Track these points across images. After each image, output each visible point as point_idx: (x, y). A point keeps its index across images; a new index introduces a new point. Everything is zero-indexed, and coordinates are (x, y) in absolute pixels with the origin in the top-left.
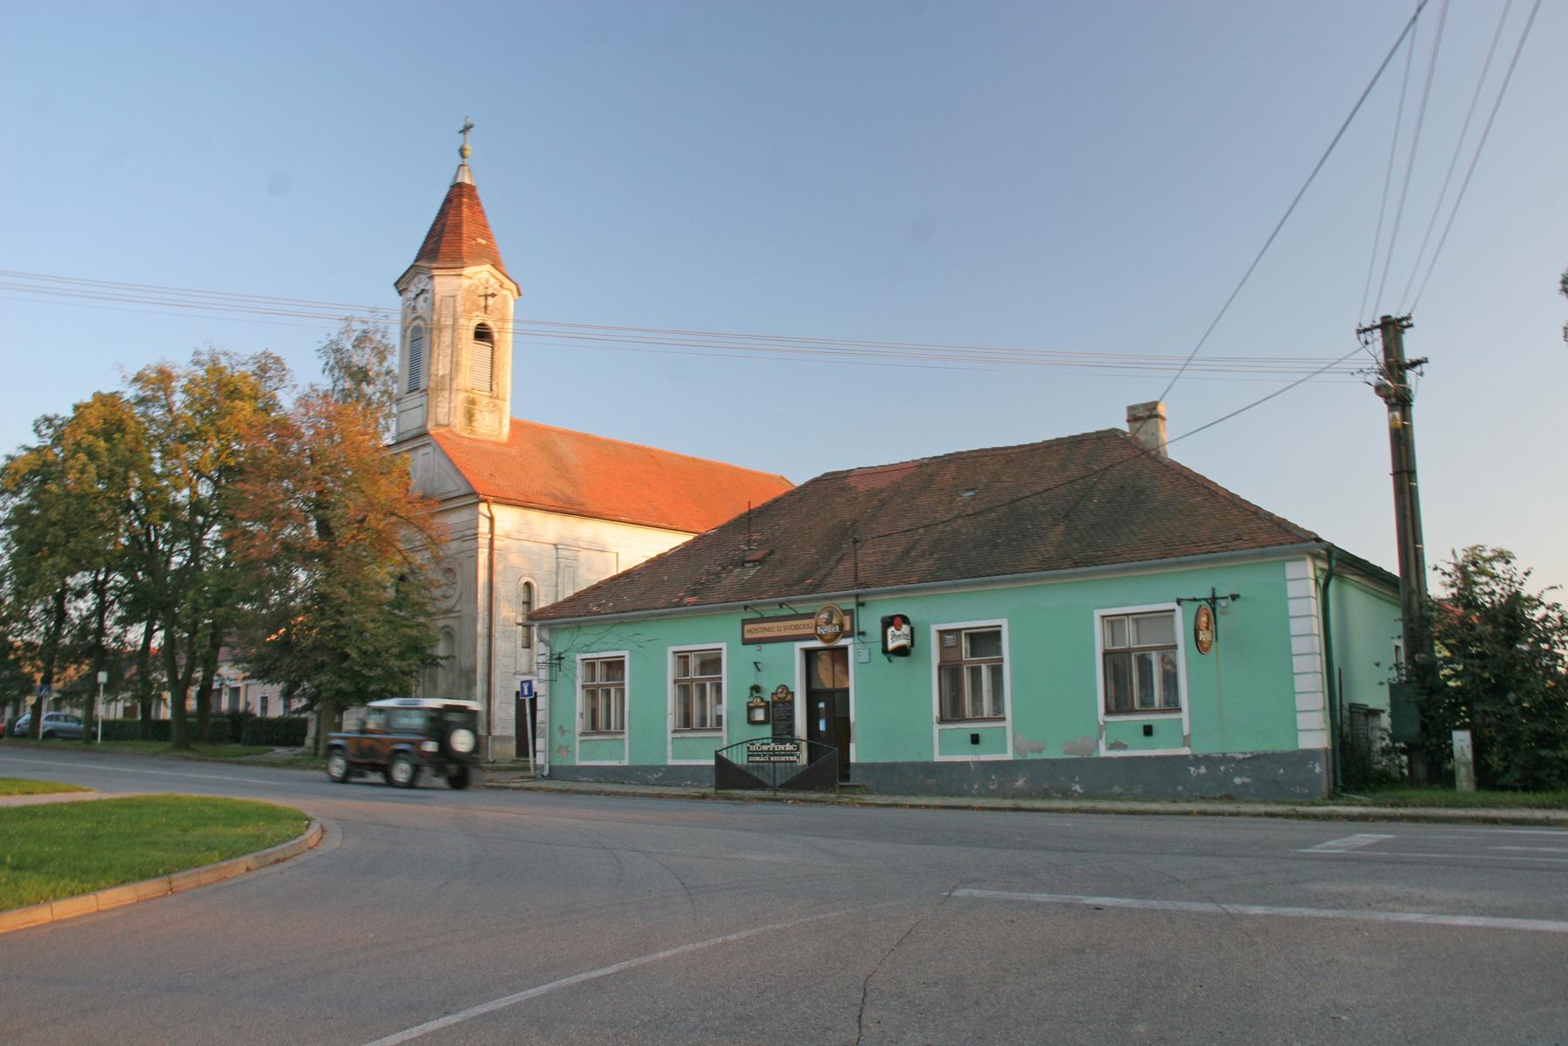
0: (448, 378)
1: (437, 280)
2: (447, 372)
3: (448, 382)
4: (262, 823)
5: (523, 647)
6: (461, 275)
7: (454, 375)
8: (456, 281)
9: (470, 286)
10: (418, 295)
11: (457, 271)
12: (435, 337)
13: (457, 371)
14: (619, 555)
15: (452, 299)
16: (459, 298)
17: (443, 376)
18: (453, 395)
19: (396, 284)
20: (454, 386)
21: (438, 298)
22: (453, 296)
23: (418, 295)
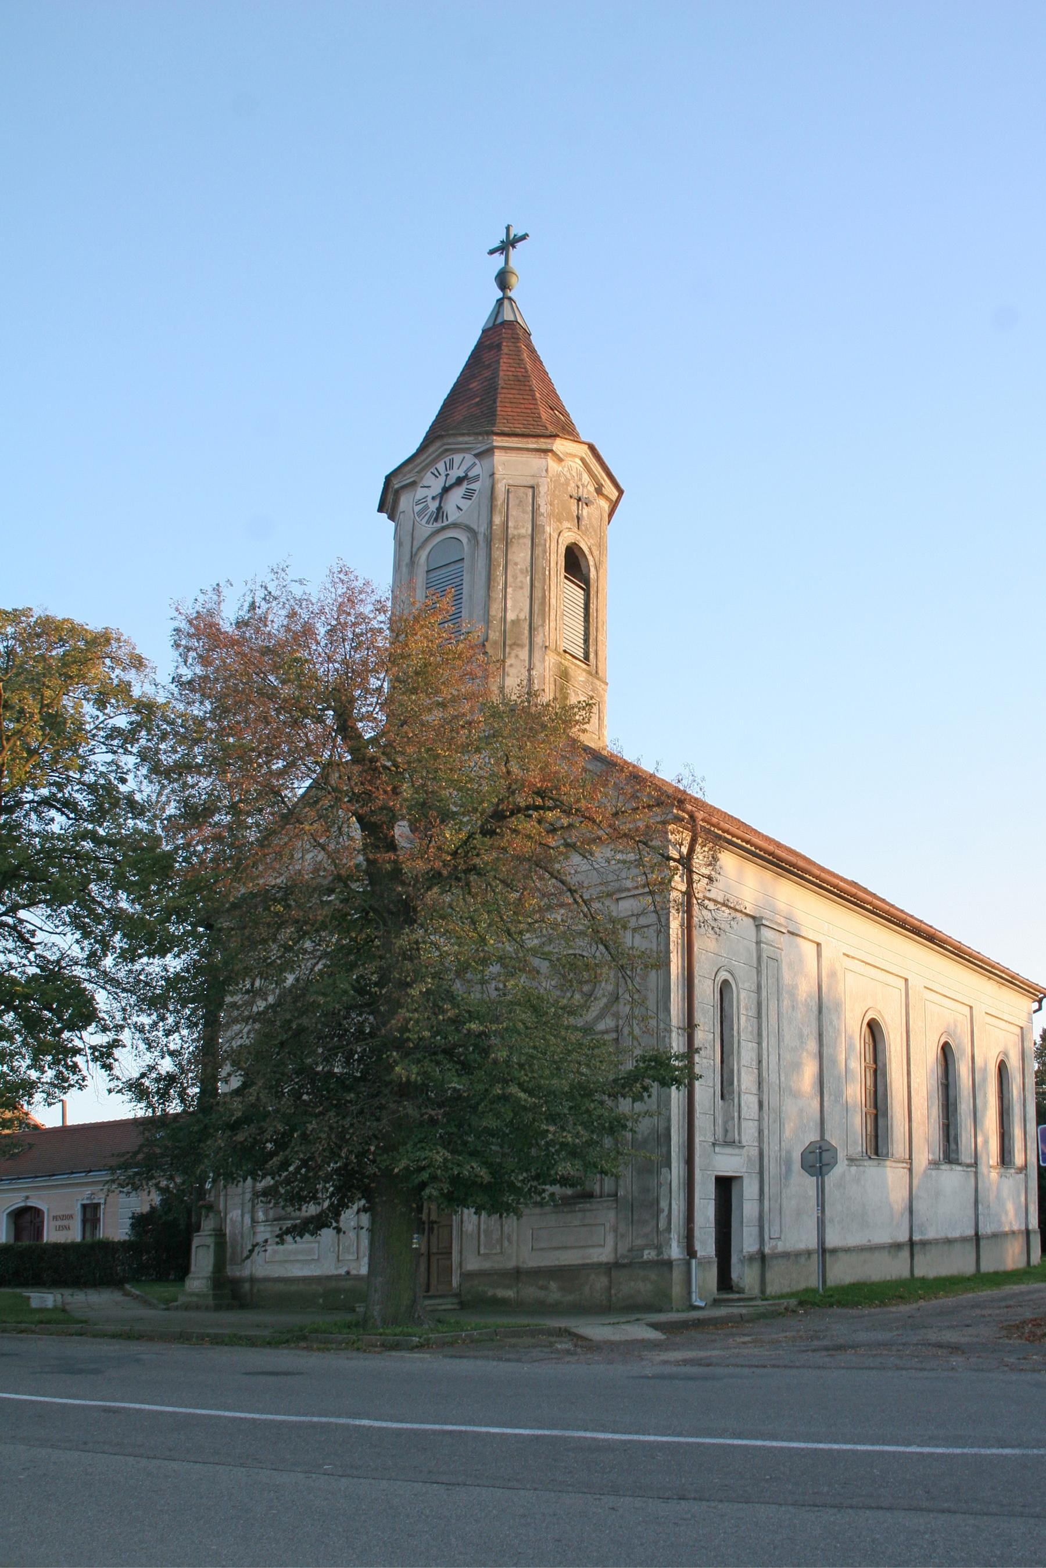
0: (526, 626)
1: (499, 457)
2: (525, 614)
3: (526, 632)
4: (220, 1040)
5: (740, 1178)
6: (546, 451)
7: (537, 620)
8: (536, 462)
9: (559, 475)
10: (446, 490)
11: (543, 443)
12: (497, 554)
13: (543, 614)
14: (1024, 1030)
15: (530, 490)
16: (543, 489)
17: (516, 623)
18: (537, 655)
19: (380, 509)
20: (538, 639)
21: (501, 488)
22: (533, 487)
23: (446, 490)
